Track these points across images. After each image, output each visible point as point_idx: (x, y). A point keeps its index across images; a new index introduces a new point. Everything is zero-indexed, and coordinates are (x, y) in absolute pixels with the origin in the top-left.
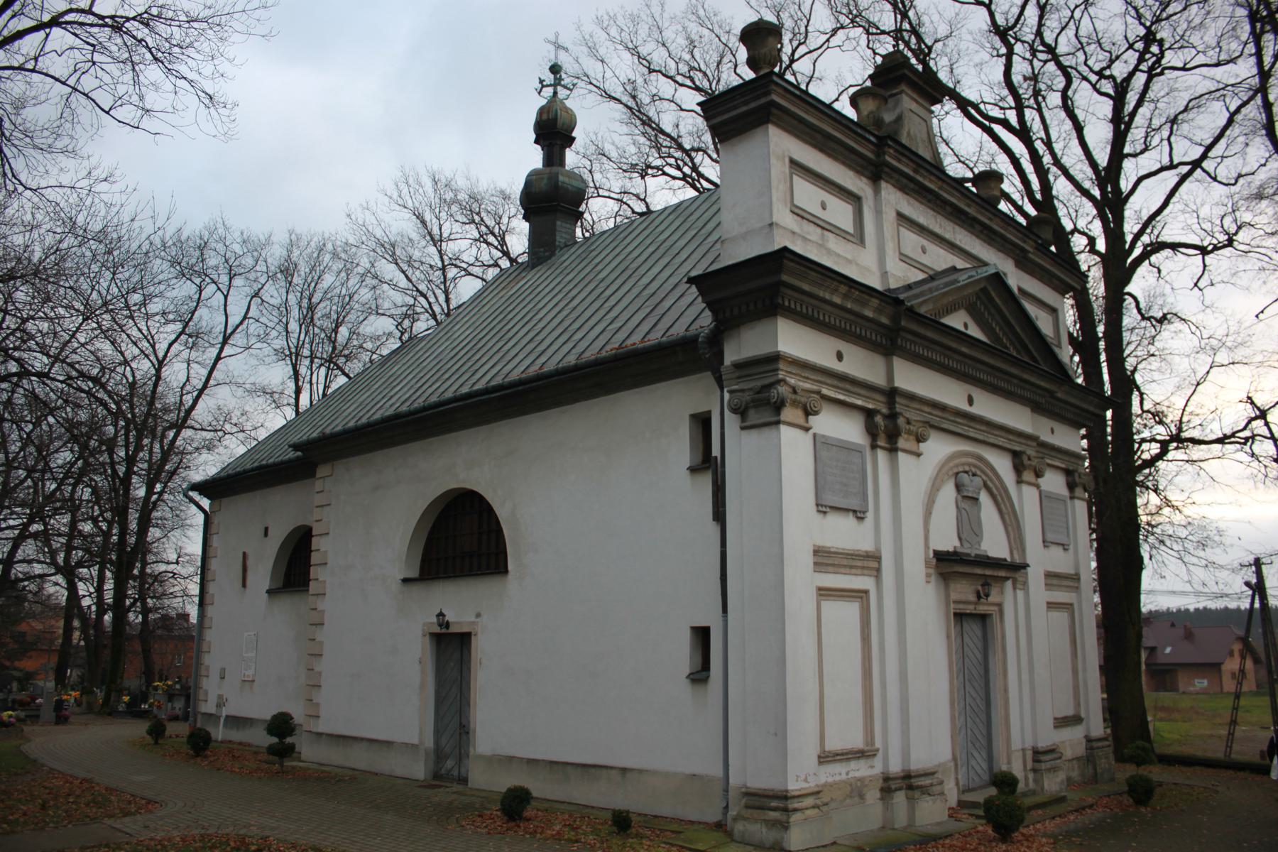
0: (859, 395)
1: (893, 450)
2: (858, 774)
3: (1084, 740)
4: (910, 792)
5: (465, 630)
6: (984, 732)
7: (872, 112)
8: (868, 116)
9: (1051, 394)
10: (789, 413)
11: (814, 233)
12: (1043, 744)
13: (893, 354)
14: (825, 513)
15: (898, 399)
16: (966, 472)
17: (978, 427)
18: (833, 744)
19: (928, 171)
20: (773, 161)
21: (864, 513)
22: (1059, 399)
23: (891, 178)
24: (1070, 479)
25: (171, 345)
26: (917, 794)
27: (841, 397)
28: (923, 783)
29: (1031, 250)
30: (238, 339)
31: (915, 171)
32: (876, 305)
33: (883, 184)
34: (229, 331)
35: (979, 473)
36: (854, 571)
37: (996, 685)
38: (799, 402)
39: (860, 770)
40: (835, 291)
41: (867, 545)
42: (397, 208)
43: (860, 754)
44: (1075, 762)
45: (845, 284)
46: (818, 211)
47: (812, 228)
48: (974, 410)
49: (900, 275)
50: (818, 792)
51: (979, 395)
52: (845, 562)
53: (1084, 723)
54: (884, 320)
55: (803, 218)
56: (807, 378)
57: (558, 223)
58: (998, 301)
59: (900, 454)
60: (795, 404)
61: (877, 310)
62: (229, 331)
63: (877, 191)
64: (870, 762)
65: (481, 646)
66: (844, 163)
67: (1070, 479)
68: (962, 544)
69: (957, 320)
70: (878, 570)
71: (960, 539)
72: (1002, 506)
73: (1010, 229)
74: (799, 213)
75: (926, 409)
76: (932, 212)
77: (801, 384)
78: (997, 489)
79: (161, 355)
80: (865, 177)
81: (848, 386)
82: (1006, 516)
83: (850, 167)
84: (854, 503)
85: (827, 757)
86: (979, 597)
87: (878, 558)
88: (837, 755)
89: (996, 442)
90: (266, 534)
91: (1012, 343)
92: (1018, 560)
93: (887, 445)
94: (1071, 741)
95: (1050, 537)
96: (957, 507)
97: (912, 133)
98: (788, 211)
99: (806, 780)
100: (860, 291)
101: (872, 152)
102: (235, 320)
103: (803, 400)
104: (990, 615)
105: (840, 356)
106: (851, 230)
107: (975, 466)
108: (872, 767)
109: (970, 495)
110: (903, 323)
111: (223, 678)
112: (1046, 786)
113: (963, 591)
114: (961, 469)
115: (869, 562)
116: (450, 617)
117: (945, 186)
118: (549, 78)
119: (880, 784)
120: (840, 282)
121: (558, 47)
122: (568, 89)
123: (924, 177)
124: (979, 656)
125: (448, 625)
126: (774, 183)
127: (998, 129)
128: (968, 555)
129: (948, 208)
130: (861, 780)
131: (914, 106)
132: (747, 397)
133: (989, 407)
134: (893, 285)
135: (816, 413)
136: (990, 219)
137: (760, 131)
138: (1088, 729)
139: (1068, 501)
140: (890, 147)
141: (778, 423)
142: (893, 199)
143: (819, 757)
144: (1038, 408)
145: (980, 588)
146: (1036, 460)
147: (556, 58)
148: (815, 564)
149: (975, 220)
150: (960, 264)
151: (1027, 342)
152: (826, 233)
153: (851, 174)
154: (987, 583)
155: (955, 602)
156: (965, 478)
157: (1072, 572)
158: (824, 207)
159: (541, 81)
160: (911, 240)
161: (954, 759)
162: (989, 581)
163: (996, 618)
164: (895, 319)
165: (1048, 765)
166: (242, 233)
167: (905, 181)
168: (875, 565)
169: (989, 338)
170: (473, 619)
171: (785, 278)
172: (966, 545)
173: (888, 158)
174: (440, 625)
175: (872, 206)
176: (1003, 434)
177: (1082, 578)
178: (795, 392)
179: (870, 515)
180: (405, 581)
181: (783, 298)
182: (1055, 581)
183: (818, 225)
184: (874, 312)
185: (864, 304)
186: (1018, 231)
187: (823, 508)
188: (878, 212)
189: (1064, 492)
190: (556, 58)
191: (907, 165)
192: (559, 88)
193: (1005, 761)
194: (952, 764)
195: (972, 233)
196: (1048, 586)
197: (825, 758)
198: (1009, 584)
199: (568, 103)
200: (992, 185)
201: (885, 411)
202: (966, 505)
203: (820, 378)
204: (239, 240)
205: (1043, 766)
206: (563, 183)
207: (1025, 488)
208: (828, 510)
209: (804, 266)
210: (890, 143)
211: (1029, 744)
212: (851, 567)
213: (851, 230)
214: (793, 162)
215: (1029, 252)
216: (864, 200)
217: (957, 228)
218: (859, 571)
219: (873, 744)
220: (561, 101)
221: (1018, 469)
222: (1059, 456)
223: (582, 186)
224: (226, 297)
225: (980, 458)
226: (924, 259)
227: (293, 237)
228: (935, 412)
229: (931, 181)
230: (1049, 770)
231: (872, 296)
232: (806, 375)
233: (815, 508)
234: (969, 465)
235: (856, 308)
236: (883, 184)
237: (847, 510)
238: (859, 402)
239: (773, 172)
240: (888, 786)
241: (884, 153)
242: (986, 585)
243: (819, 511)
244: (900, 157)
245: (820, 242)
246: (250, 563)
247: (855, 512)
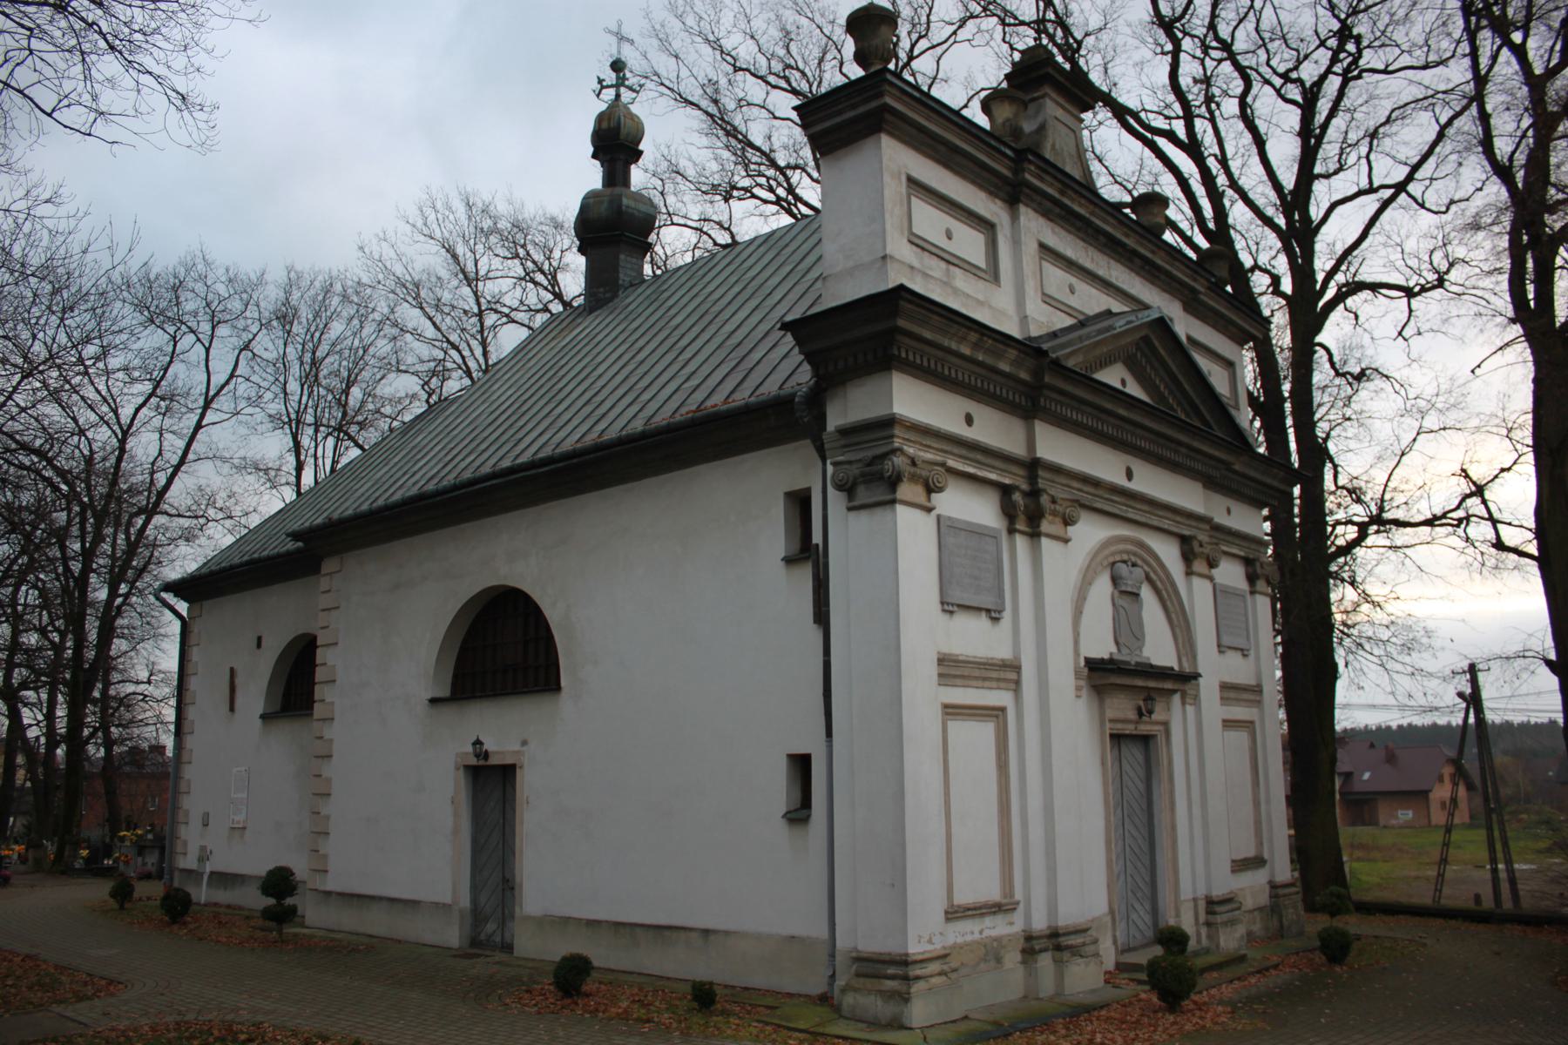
0: (993, 467)
1: (1034, 535)
2: (994, 933)
3: (1267, 888)
4: (1058, 954)
5: (509, 761)
6: (1147, 879)
7: (1008, 120)
8: (1004, 124)
9: (1228, 466)
10: (906, 490)
11: (937, 268)
12: (1218, 892)
13: (1034, 418)
14: (951, 613)
15: (1041, 473)
16: (1125, 562)
17: (1139, 506)
18: (963, 897)
19: (1076, 192)
20: (887, 178)
21: (1000, 612)
22: (1235, 472)
23: (1033, 200)
24: (1250, 570)
25: (137, 410)
26: (1066, 955)
27: (971, 470)
28: (1070, 943)
29: (1202, 290)
30: (223, 402)
31: (1062, 193)
32: (1013, 357)
33: (1022, 209)
34: (212, 393)
35: (1139, 562)
36: (987, 684)
37: (1161, 818)
38: (920, 477)
39: (997, 927)
40: (963, 339)
41: (1003, 652)
42: (422, 238)
43: (997, 909)
44: (1256, 913)
45: (976, 331)
46: (942, 242)
47: (935, 262)
48: (1135, 486)
49: (1042, 320)
50: (945, 956)
51: (1139, 467)
52: (977, 673)
53: (1267, 866)
54: (1024, 375)
55: (923, 249)
56: (929, 447)
57: (622, 257)
58: (1162, 352)
59: (1045, 541)
60: (914, 478)
61: (1013, 363)
62: (212, 393)
63: (1014, 217)
64: (1008, 917)
65: (529, 782)
66: (973, 182)
67: (1250, 570)
68: (1119, 650)
69: (1113, 376)
70: (1018, 683)
71: (1117, 643)
72: (1168, 603)
73: (1177, 264)
74: (919, 243)
75: (1075, 484)
76: (1082, 244)
77: (921, 454)
79: (125, 420)
80: (1000, 199)
81: (979, 457)
82: (1173, 616)
83: (981, 187)
84: (987, 601)
85: (956, 912)
86: (1141, 714)
87: (1016, 667)
88: (969, 909)
89: (1161, 525)
90: (259, 645)
91: (1179, 404)
92: (1187, 669)
93: (1027, 529)
94: (1252, 887)
95: (1226, 640)
96: (1114, 604)
97: (1057, 146)
98: (905, 241)
99: (930, 941)
100: (994, 339)
101: (1009, 168)
102: (218, 379)
103: (924, 473)
104: (1154, 736)
105: (969, 420)
106: (983, 265)
107: (1135, 554)
108: (1012, 924)
109: (1129, 589)
110: (1047, 379)
111: (205, 825)
112: (1222, 943)
113: (1122, 707)
114: (1118, 558)
115: (1006, 672)
116: (489, 745)
117: (1097, 210)
118: (610, 77)
119: (1021, 943)
120: (970, 329)
121: (621, 38)
122: (634, 91)
123: (1073, 200)
124: (1141, 787)
125: (486, 755)
126: (888, 205)
127: (1162, 142)
128: (1128, 663)
129: (1102, 238)
130: (998, 939)
131: (1060, 113)
132: (855, 470)
133: (1152, 482)
134: (1035, 332)
135: (940, 490)
136: (1153, 252)
137: (870, 142)
138: (1272, 874)
139: (1248, 596)
140: (1030, 162)
141: (893, 502)
142: (1034, 227)
143: (946, 913)
144: (1212, 483)
145: (1141, 703)
146: (1209, 547)
147: (619, 52)
148: (940, 675)
149: (1135, 253)
150: (1117, 307)
151: (1197, 401)
152: (952, 268)
153: (982, 195)
154: (1150, 696)
155: (1111, 721)
156: (1123, 570)
157: (1253, 682)
158: (949, 236)
159: (600, 81)
160: (1057, 278)
161: (1112, 912)
162: (1153, 695)
163: (1161, 739)
164: (1037, 373)
165: (1225, 917)
166: (227, 270)
167: (1049, 205)
168: (1013, 676)
169: (1152, 398)
170: (517, 747)
171: (901, 323)
172: (1125, 651)
173: (1028, 176)
174: (477, 756)
175: (1009, 235)
176: (1169, 515)
177: (1265, 689)
178: (914, 463)
179: (1007, 615)
180: (434, 701)
181: (899, 349)
182: (1232, 694)
183: (943, 259)
184: (1011, 365)
185: (999, 356)
186: (1188, 267)
187: (949, 607)
188: (1016, 242)
189: (1243, 585)
190: (619, 52)
191: (1051, 185)
192: (623, 90)
193: (1173, 913)
194: (1108, 919)
195: (1132, 270)
196: (1224, 700)
197: (955, 913)
198: (1177, 698)
199: (634, 109)
200: (1155, 211)
201: (1025, 486)
202: (1124, 602)
203: (945, 447)
204: (223, 279)
205: (1219, 919)
206: (628, 207)
207: (1196, 581)
208: (955, 608)
209: (924, 308)
210: (1030, 157)
211: (1201, 892)
212: (985, 679)
213: (983, 265)
214: (912, 181)
215: (1200, 293)
216: (999, 228)
217: (1112, 262)
218: (994, 684)
219: (1012, 896)
220: (625, 106)
221: (1188, 557)
222: (1237, 541)
223: (651, 211)
224: (208, 350)
225: (1142, 545)
226: (1073, 301)
227: (292, 275)
228: (1086, 488)
229: (1081, 205)
230: (1225, 924)
231: (1008, 346)
232: (928, 443)
233: (939, 606)
234: (1128, 552)
235: (989, 360)
236: (1022, 209)
237: (979, 609)
238: (993, 476)
239: (887, 192)
240: (1031, 946)
241: (1023, 170)
242: (1149, 699)
243: (944, 611)
244: (1044, 175)
245: (945, 279)
246: (238, 681)
247: (988, 611)
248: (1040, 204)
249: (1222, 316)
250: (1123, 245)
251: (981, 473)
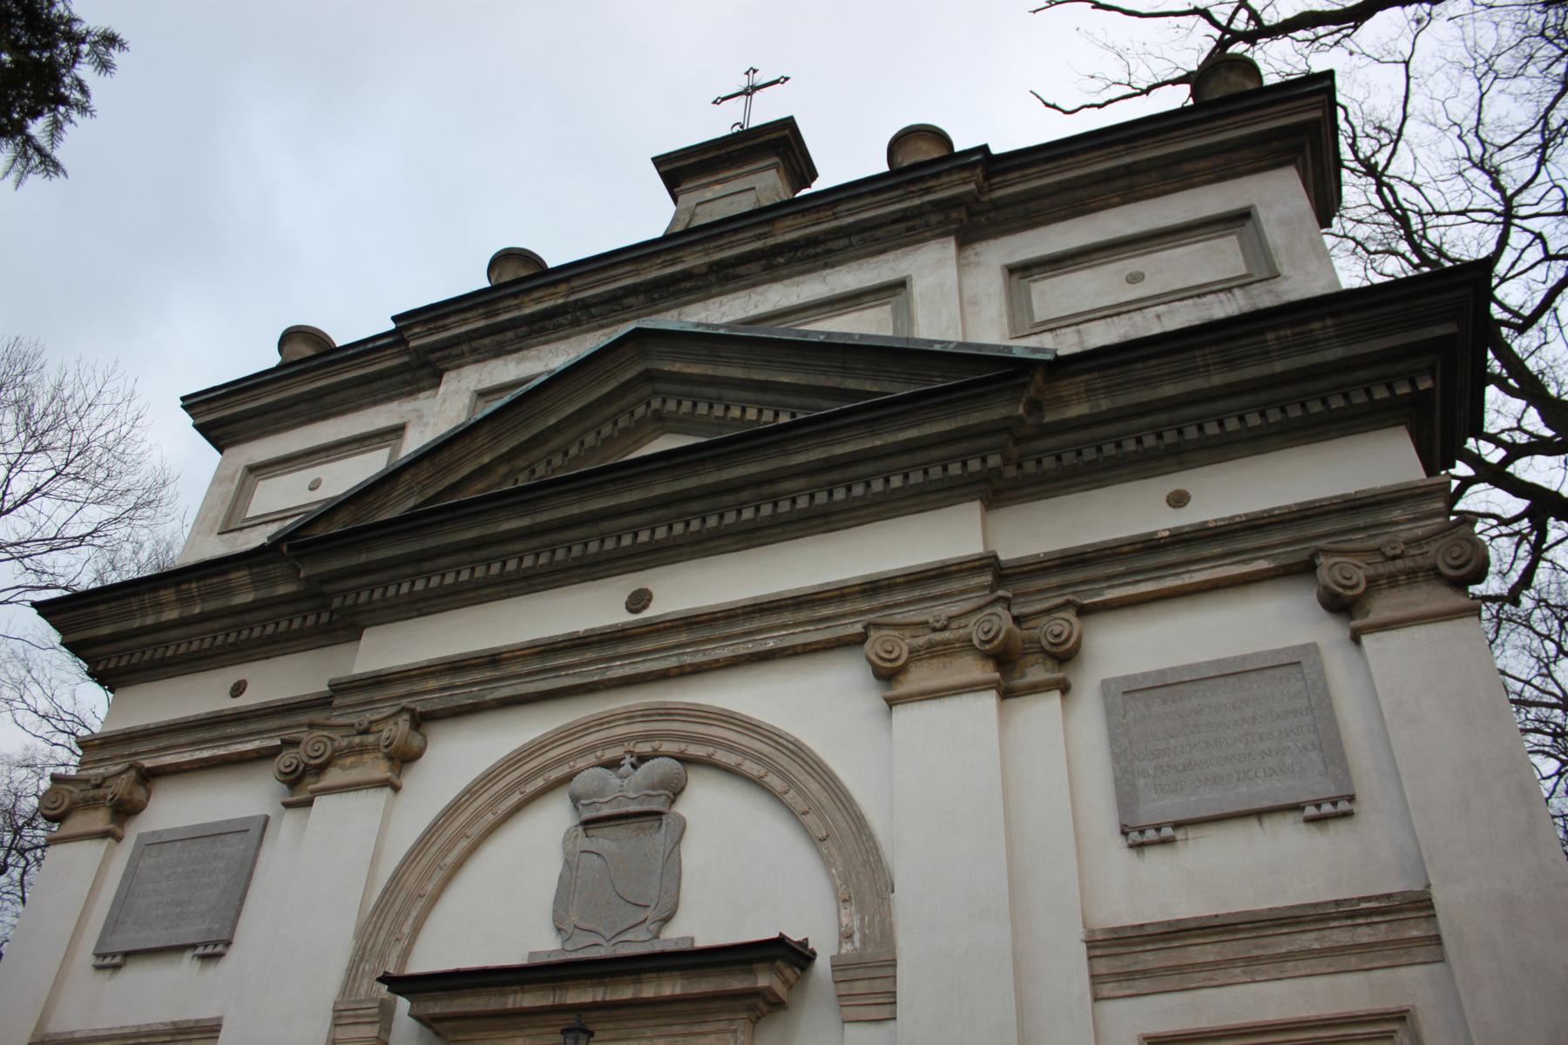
17: (649, 646)
19: (516, 295)
23: (462, 354)
31: (487, 316)
32: (247, 580)
40: (159, 606)
54: (283, 589)
61: (255, 584)
66: (375, 403)
75: (432, 684)
78: (758, 758)
100: (199, 579)
101: (400, 354)
107: (647, 737)
109: (606, 811)
120: (156, 589)
123: (518, 307)
184: (256, 589)
185: (229, 591)
189: (1327, 633)
202: (604, 841)
225: (667, 713)
229: (539, 300)
235: (212, 605)
237: (180, 949)
244: (441, 323)
248: (474, 351)
249: (1129, 170)
250: (686, 275)
251: (222, 752)
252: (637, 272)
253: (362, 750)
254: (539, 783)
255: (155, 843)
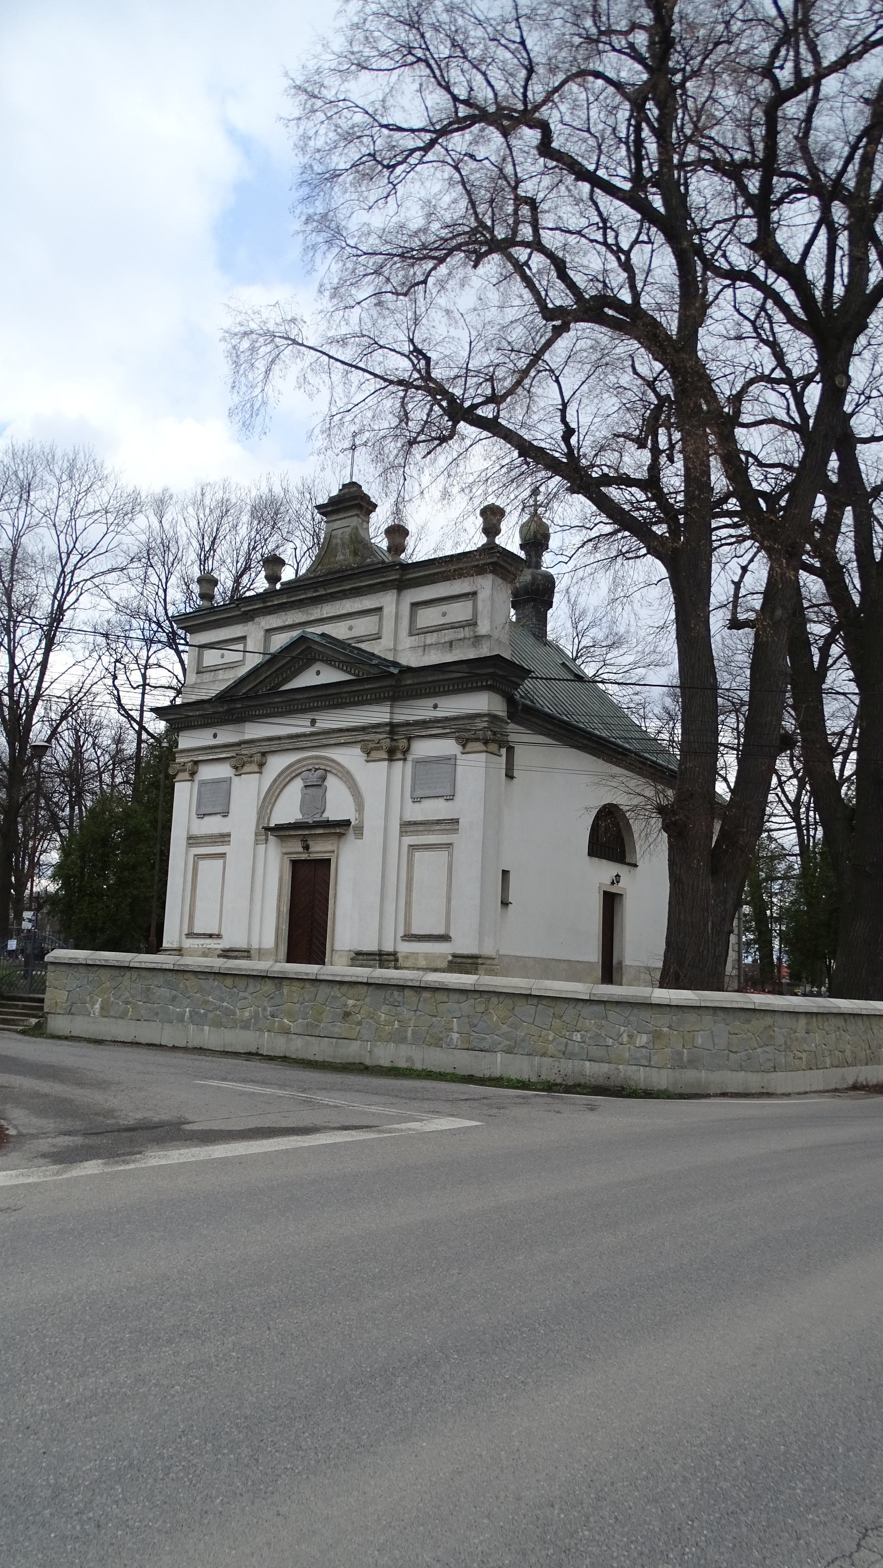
27: (211, 757)
83: (238, 623)
89: (338, 742)
128: (307, 823)
176: (346, 734)
202: (310, 791)
212: (215, 842)
252: (306, 594)
253: (251, 762)
254: (294, 774)
255: (203, 783)
